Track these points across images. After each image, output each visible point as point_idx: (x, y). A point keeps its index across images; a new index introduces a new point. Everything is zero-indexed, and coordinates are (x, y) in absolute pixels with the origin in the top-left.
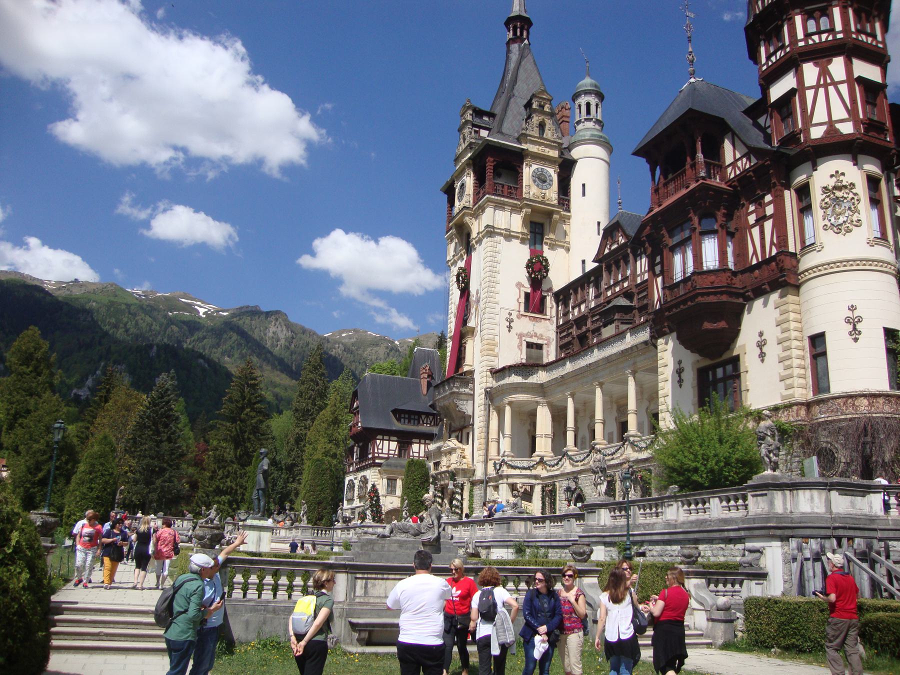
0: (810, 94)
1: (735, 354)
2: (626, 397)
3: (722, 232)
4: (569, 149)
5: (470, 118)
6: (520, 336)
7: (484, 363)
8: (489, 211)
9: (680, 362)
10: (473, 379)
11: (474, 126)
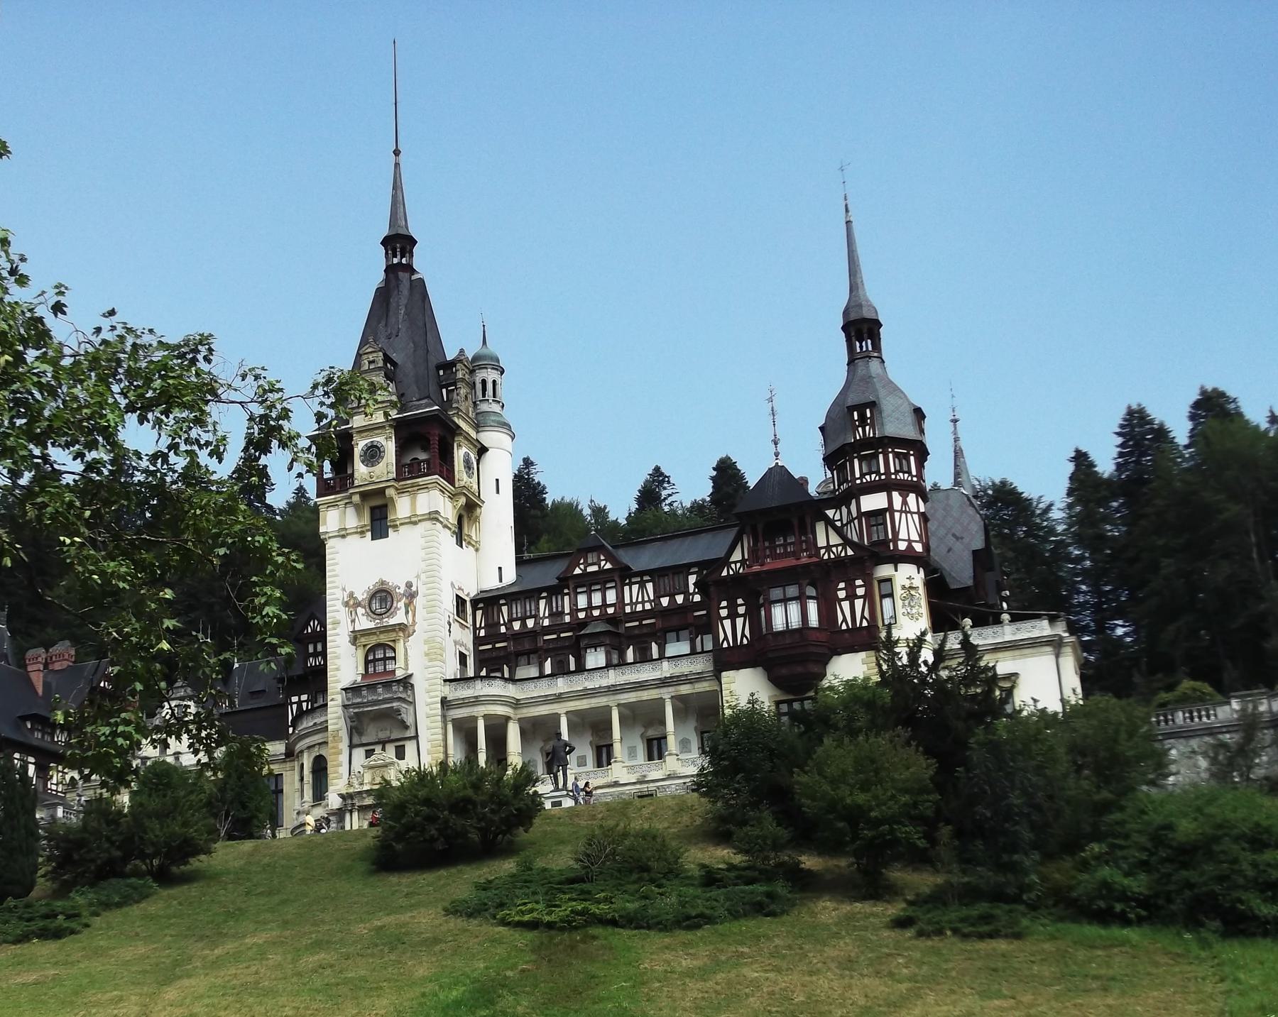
0: (897, 515)
6: (456, 643)
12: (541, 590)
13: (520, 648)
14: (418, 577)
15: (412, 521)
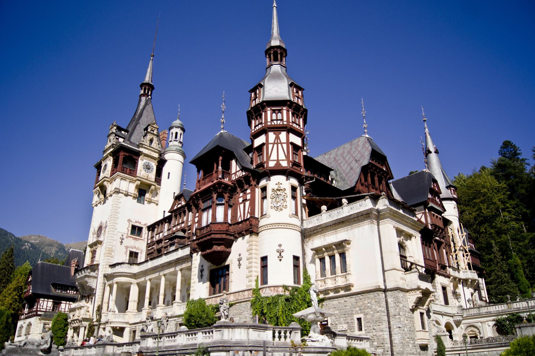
0: (270, 146)
1: (227, 263)
2: (176, 283)
3: (227, 205)
4: (164, 154)
5: (114, 131)
6: (127, 247)
7: (105, 261)
8: (118, 180)
9: (202, 266)
10: (98, 269)
11: (116, 135)
13: (158, 247)
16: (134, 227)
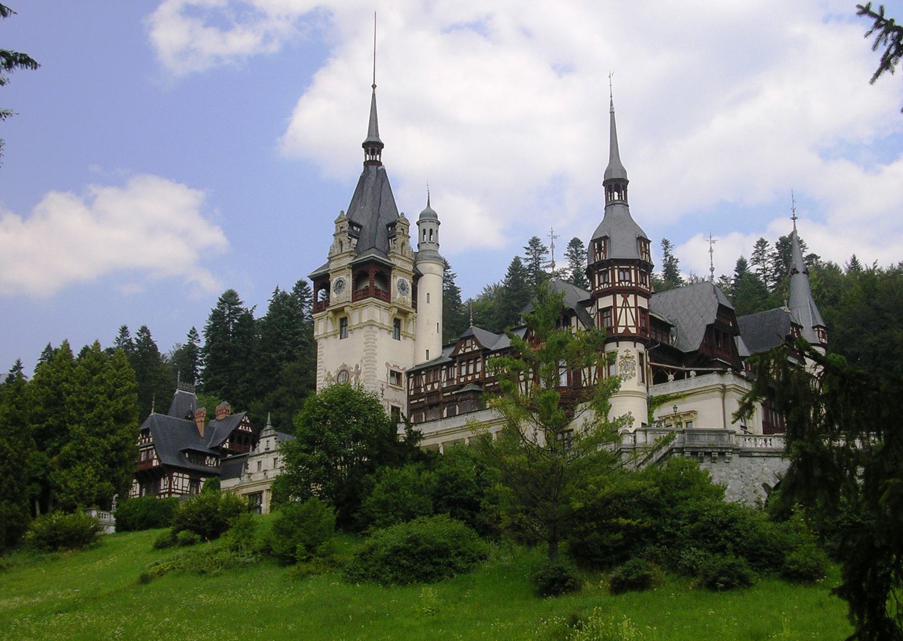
0: (619, 310)
12: (442, 365)
13: (431, 402)
14: (362, 361)
15: (361, 327)
16: (393, 373)
